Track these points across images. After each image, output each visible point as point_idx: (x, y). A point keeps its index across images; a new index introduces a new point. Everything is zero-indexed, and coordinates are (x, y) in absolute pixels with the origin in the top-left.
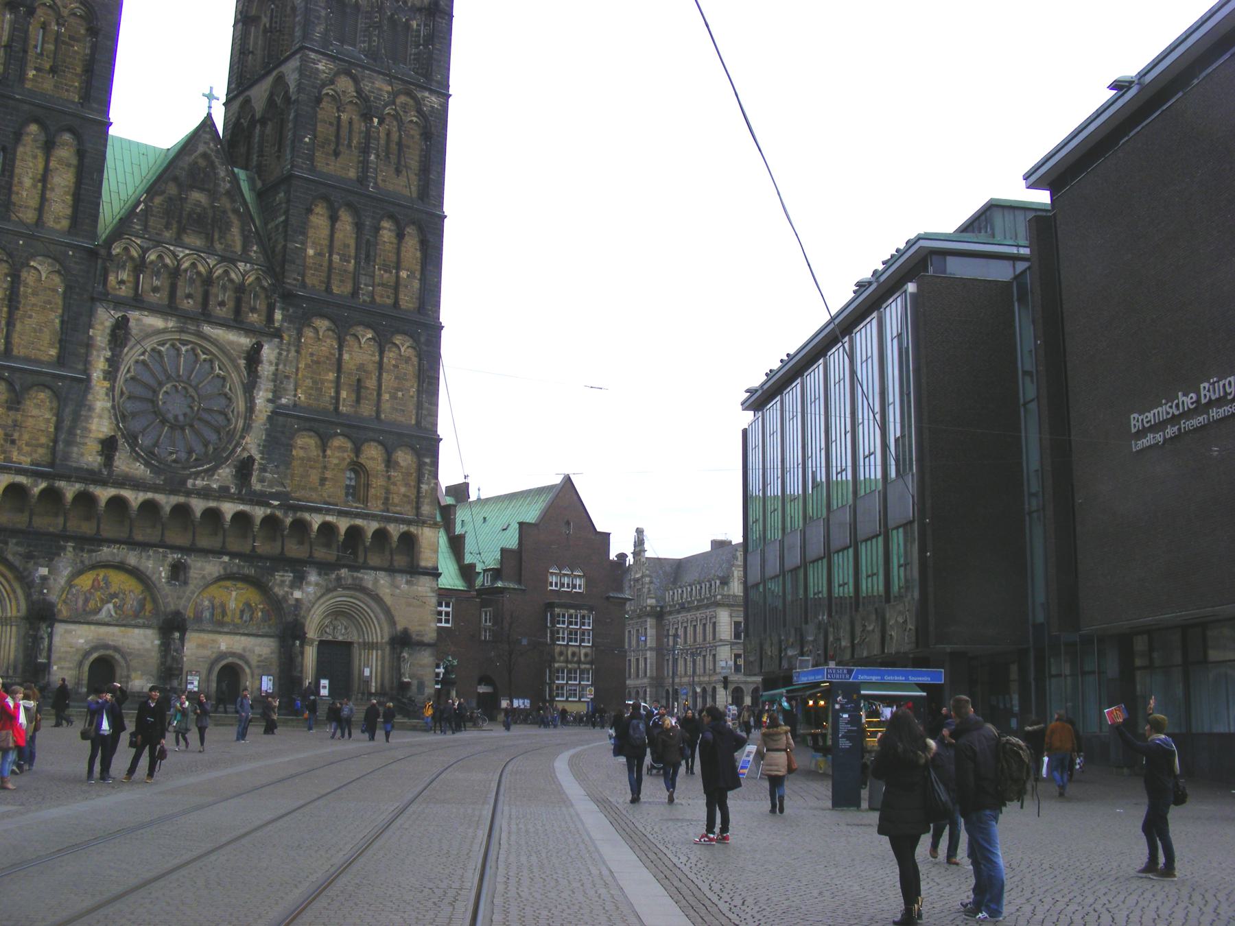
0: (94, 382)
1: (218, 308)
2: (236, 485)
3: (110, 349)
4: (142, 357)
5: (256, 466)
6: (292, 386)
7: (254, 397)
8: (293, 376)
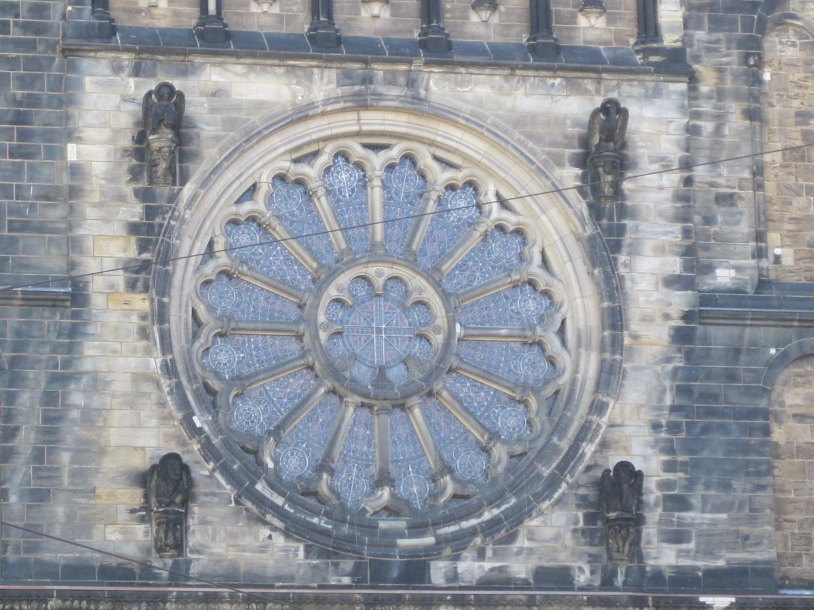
0: (98, 300)
1: (474, 17)
2: (593, 559)
3: (144, 195)
4: (247, 207)
5: (652, 492)
6: (745, 227)
7: (621, 278)
8: (748, 194)
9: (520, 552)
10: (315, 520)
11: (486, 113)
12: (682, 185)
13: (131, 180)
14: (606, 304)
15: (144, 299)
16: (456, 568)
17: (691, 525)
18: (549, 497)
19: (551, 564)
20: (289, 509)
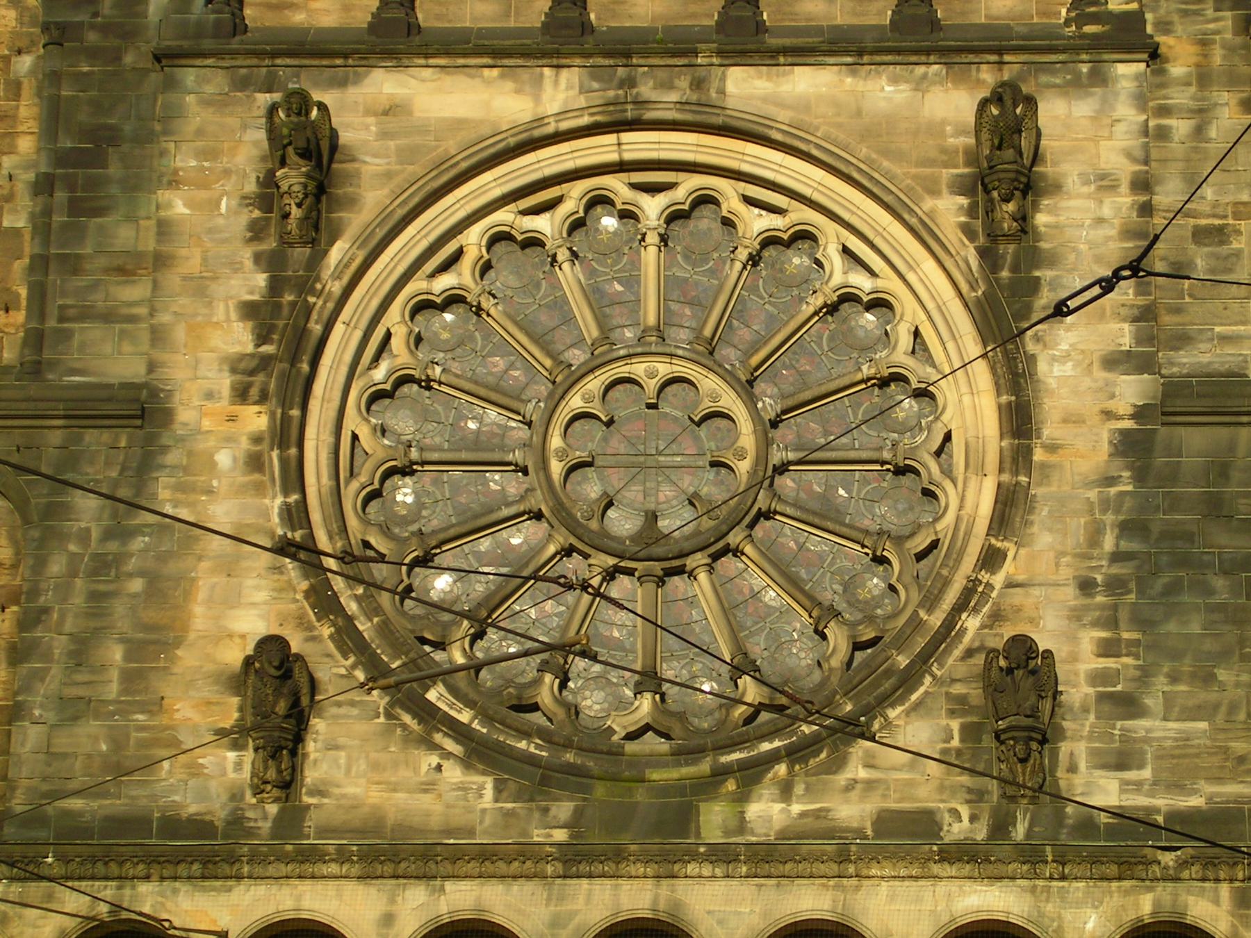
0: (185, 416)
2: (976, 797)
7: (1032, 359)
9: (851, 785)
10: (523, 745)
11: (816, 122)
12: (1135, 214)
13: (251, 240)
14: (1004, 399)
15: (260, 412)
16: (743, 812)
17: (1146, 740)
18: (902, 700)
19: (906, 806)
20: (478, 727)
